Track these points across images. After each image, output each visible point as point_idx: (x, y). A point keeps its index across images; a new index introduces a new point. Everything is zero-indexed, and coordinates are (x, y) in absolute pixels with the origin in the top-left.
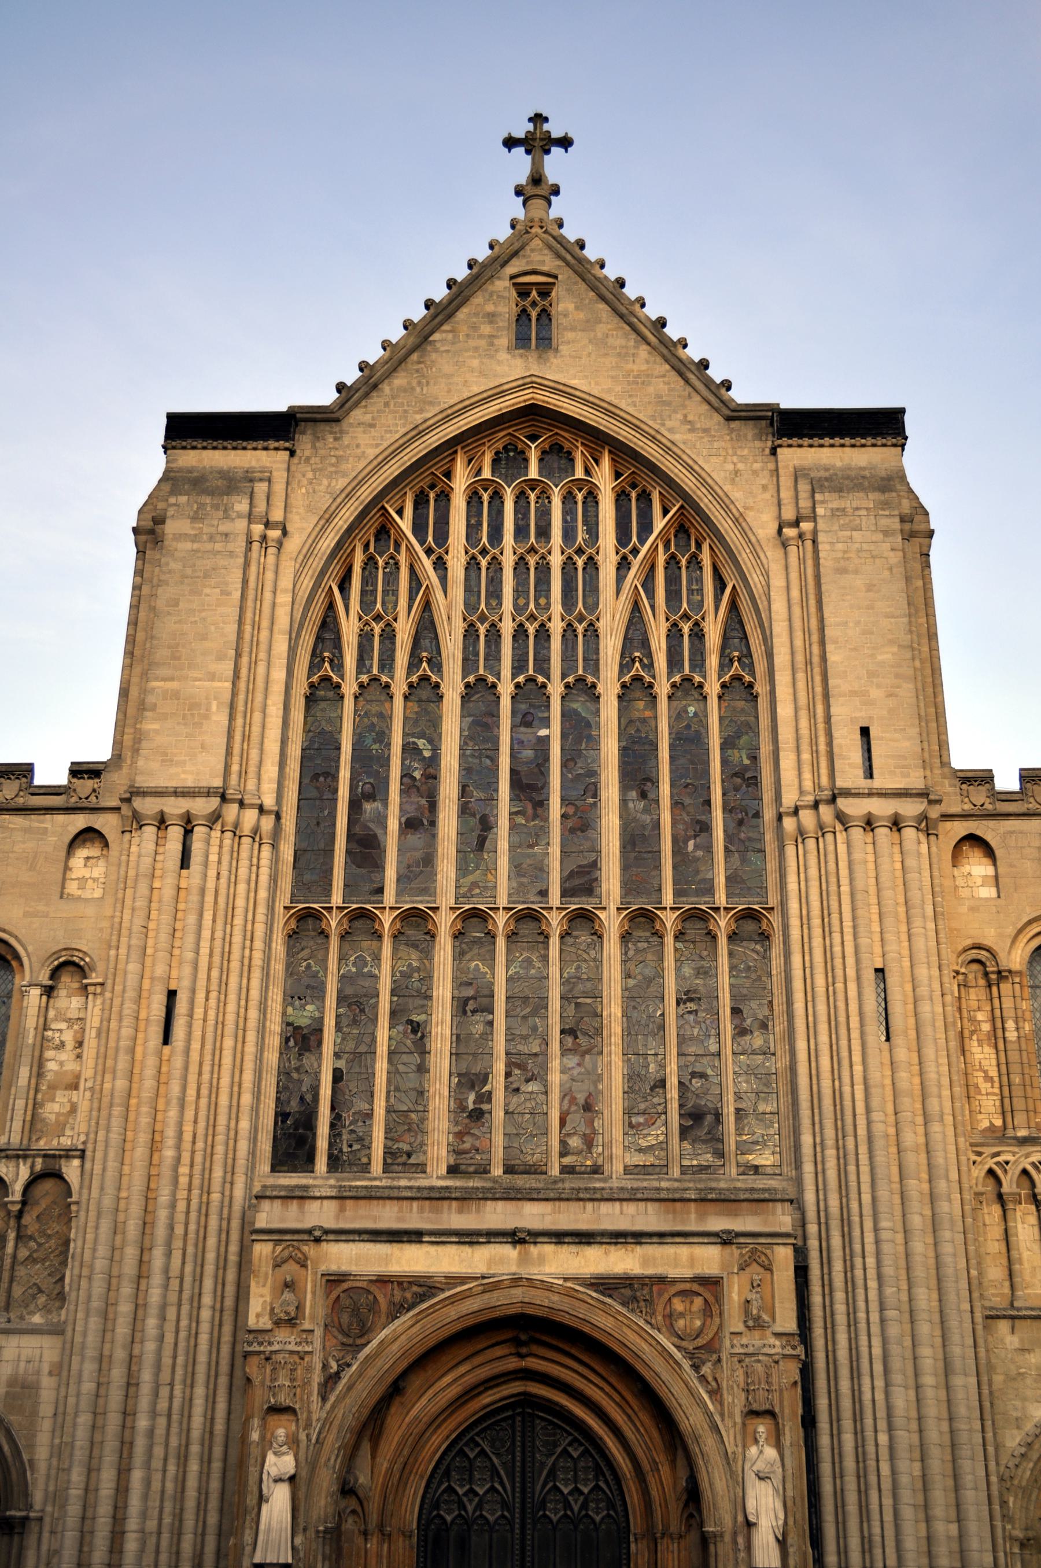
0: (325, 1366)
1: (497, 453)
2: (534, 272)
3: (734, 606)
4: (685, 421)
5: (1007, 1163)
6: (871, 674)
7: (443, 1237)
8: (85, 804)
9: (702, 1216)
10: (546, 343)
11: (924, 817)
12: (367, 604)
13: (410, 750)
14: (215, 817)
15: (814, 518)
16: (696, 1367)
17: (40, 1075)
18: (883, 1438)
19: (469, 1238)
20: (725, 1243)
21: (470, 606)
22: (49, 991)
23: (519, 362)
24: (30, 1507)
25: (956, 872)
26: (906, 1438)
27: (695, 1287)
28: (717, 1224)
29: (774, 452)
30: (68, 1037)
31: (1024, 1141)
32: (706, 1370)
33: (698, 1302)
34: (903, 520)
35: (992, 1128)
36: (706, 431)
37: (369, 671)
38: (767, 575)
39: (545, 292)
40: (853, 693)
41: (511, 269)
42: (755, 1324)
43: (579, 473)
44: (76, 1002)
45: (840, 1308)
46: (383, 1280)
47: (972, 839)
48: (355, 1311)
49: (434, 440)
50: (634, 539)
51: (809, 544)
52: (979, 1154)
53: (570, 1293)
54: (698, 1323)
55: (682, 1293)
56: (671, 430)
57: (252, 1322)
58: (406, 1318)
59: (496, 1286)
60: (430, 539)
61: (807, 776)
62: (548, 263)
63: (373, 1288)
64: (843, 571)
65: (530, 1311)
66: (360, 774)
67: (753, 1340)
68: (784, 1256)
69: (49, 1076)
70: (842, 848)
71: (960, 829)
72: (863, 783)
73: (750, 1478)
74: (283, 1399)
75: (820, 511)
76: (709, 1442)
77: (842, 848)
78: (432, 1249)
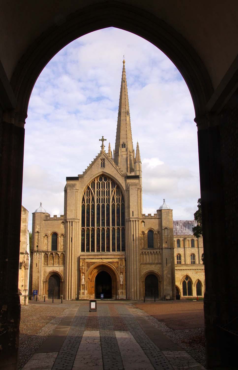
2: (102, 158)
3: (123, 195)
4: (118, 176)
6: (134, 206)
9: (117, 257)
10: (104, 166)
12: (87, 196)
15: (129, 189)
17: (61, 245)
19: (98, 259)
21: (97, 196)
22: (60, 237)
23: (101, 169)
31: (145, 249)
32: (117, 269)
34: (138, 188)
39: (104, 160)
41: (100, 158)
42: (121, 265)
43: (108, 181)
46: (91, 262)
47: (143, 221)
49: (93, 178)
53: (106, 263)
58: (93, 265)
62: (104, 157)
64: (132, 195)
68: (124, 260)
71: (142, 220)
75: (130, 188)
76: (117, 275)
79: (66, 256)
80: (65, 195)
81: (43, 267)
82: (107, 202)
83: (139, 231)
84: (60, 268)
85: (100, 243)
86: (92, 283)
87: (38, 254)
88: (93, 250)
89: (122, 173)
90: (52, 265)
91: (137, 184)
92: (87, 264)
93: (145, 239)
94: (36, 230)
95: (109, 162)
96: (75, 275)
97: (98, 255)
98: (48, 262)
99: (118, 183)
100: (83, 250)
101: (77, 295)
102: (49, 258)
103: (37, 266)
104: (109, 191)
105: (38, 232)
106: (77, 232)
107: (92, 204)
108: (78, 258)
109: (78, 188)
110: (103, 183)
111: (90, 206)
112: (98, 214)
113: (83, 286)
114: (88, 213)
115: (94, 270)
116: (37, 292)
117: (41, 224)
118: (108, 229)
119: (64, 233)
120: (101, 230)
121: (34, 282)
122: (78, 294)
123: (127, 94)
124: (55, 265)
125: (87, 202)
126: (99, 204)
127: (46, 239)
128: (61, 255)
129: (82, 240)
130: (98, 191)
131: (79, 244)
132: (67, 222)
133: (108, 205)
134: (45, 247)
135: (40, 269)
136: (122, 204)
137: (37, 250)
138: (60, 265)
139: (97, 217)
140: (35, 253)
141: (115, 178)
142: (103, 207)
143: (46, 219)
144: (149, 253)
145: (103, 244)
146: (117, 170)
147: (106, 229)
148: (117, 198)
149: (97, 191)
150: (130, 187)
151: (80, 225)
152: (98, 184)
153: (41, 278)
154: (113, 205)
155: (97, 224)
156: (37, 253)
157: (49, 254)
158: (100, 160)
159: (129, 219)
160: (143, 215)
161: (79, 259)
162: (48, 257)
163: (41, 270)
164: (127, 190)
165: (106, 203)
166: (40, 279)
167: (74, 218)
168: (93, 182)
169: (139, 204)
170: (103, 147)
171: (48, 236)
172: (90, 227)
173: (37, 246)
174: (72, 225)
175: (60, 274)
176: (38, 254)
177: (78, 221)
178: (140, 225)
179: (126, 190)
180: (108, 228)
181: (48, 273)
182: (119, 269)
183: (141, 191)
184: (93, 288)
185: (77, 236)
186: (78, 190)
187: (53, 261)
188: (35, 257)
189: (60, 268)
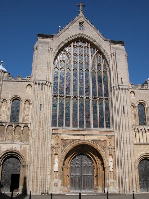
7: (75, 135)
8: (28, 81)
9: (104, 133)
11: (128, 89)
14: (45, 84)
16: (104, 150)
18: (124, 157)
19: (78, 135)
20: (107, 136)
22: (25, 104)
24: (26, 164)
26: (126, 157)
29: (110, 45)
30: (27, 110)
32: (105, 150)
35: (134, 124)
39: (82, 23)
40: (120, 74)
41: (79, 20)
44: (28, 105)
47: (132, 91)
48: (65, 143)
51: (114, 56)
59: (81, 140)
67: (110, 147)
69: (25, 114)
70: (119, 92)
71: (131, 90)
72: (122, 84)
76: (105, 158)
77: (119, 92)
84: (21, 146)
100: (54, 124)
119: (30, 98)
129: (53, 111)
145: (81, 117)
154: (93, 71)
157: (7, 126)
158: (79, 23)
171: (7, 101)
181: (3, 152)
189: (22, 147)
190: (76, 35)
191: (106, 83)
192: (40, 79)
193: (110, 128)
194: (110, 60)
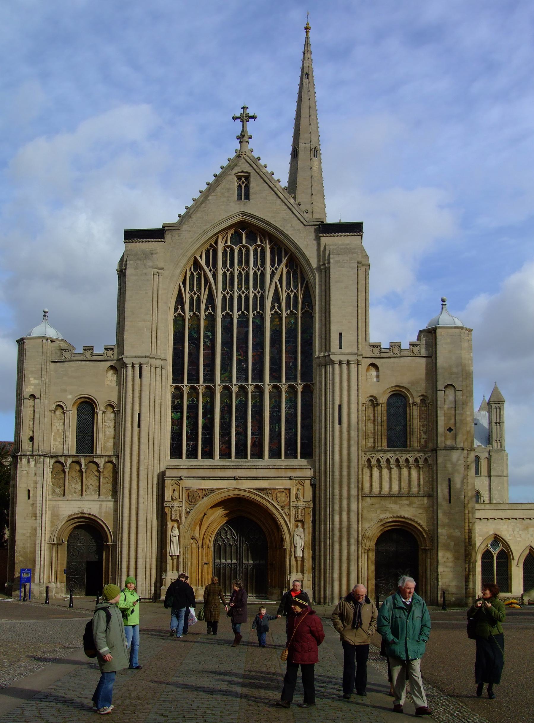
0: (186, 510)
1: (232, 234)
4: (292, 226)
5: (373, 457)
10: (247, 198)
12: (192, 289)
13: (206, 336)
15: (329, 263)
21: (224, 289)
22: (104, 412)
25: (368, 374)
27: (283, 490)
28: (290, 474)
33: (284, 494)
36: (298, 230)
37: (193, 311)
38: (315, 279)
43: (259, 243)
45: (323, 494)
46: (199, 489)
50: (276, 264)
52: (366, 454)
53: (250, 492)
54: (284, 499)
55: (279, 492)
56: (287, 230)
57: (166, 499)
58: (206, 499)
59: (230, 490)
60: (211, 266)
61: (324, 346)
63: (197, 491)
65: (239, 496)
66: (191, 344)
68: (308, 483)
71: (370, 361)
73: (295, 535)
74: (175, 518)
75: (332, 261)
78: (213, 481)
79: (120, 468)
80: (120, 284)
81: (49, 500)
82: (255, 309)
83: (360, 395)
85: (230, 433)
86: (202, 553)
87: (34, 462)
88: (208, 454)
89: (305, 217)
90: (77, 497)
91: (355, 249)
92: (188, 495)
93: (379, 421)
94: (27, 390)
95: (265, 184)
96: (149, 527)
97: (222, 468)
98: (64, 487)
99: (292, 247)
101: (156, 583)
102: (67, 474)
103: (29, 498)
104: (263, 275)
105: (33, 396)
106: (158, 398)
107: (207, 313)
108: (158, 476)
109: (161, 265)
110: (244, 250)
111: (199, 320)
112: (227, 344)
113: (175, 561)
114: (194, 341)
115: (210, 511)
116: (31, 571)
117: (44, 373)
118: (259, 391)
119: (114, 399)
120: (237, 393)
121: (22, 545)
122: (158, 585)
123: (316, 106)
124: (85, 497)
125: (191, 309)
126: (230, 313)
127: (60, 419)
128: (104, 466)
130: (228, 274)
131: (162, 434)
132: (125, 366)
133: (260, 317)
134: (57, 443)
135: (39, 505)
136: (302, 314)
137: (30, 449)
138: (101, 497)
139: (222, 354)
140: (24, 460)
141: (282, 232)
142: (243, 321)
143: (58, 359)
144: (392, 461)
146: (288, 207)
147: (250, 389)
148: (288, 296)
149: (224, 274)
150: (331, 256)
151: (167, 379)
152: (229, 253)
153: (43, 532)
154: (277, 317)
155: (221, 374)
156: (31, 460)
157: (68, 464)
159: (329, 355)
160: (372, 346)
161: (162, 478)
162: (64, 472)
163: (44, 509)
164: (322, 267)
165: (253, 311)
166: (38, 535)
167: (148, 353)
168: (211, 245)
169: (359, 311)
170: (246, 138)
171: (65, 409)
172: (198, 383)
173: (31, 439)
174: (140, 377)
175: (102, 523)
176: (32, 463)
177: (162, 362)
178: (364, 378)
179: (319, 269)
180: (257, 387)
182: (293, 512)
183: (367, 272)
184: (207, 566)
185: (158, 409)
186: (162, 269)
187: (82, 485)
188: (25, 472)
190: (228, 219)
191: (308, 343)
192: (134, 354)
193: (269, 458)
194: (317, 279)
